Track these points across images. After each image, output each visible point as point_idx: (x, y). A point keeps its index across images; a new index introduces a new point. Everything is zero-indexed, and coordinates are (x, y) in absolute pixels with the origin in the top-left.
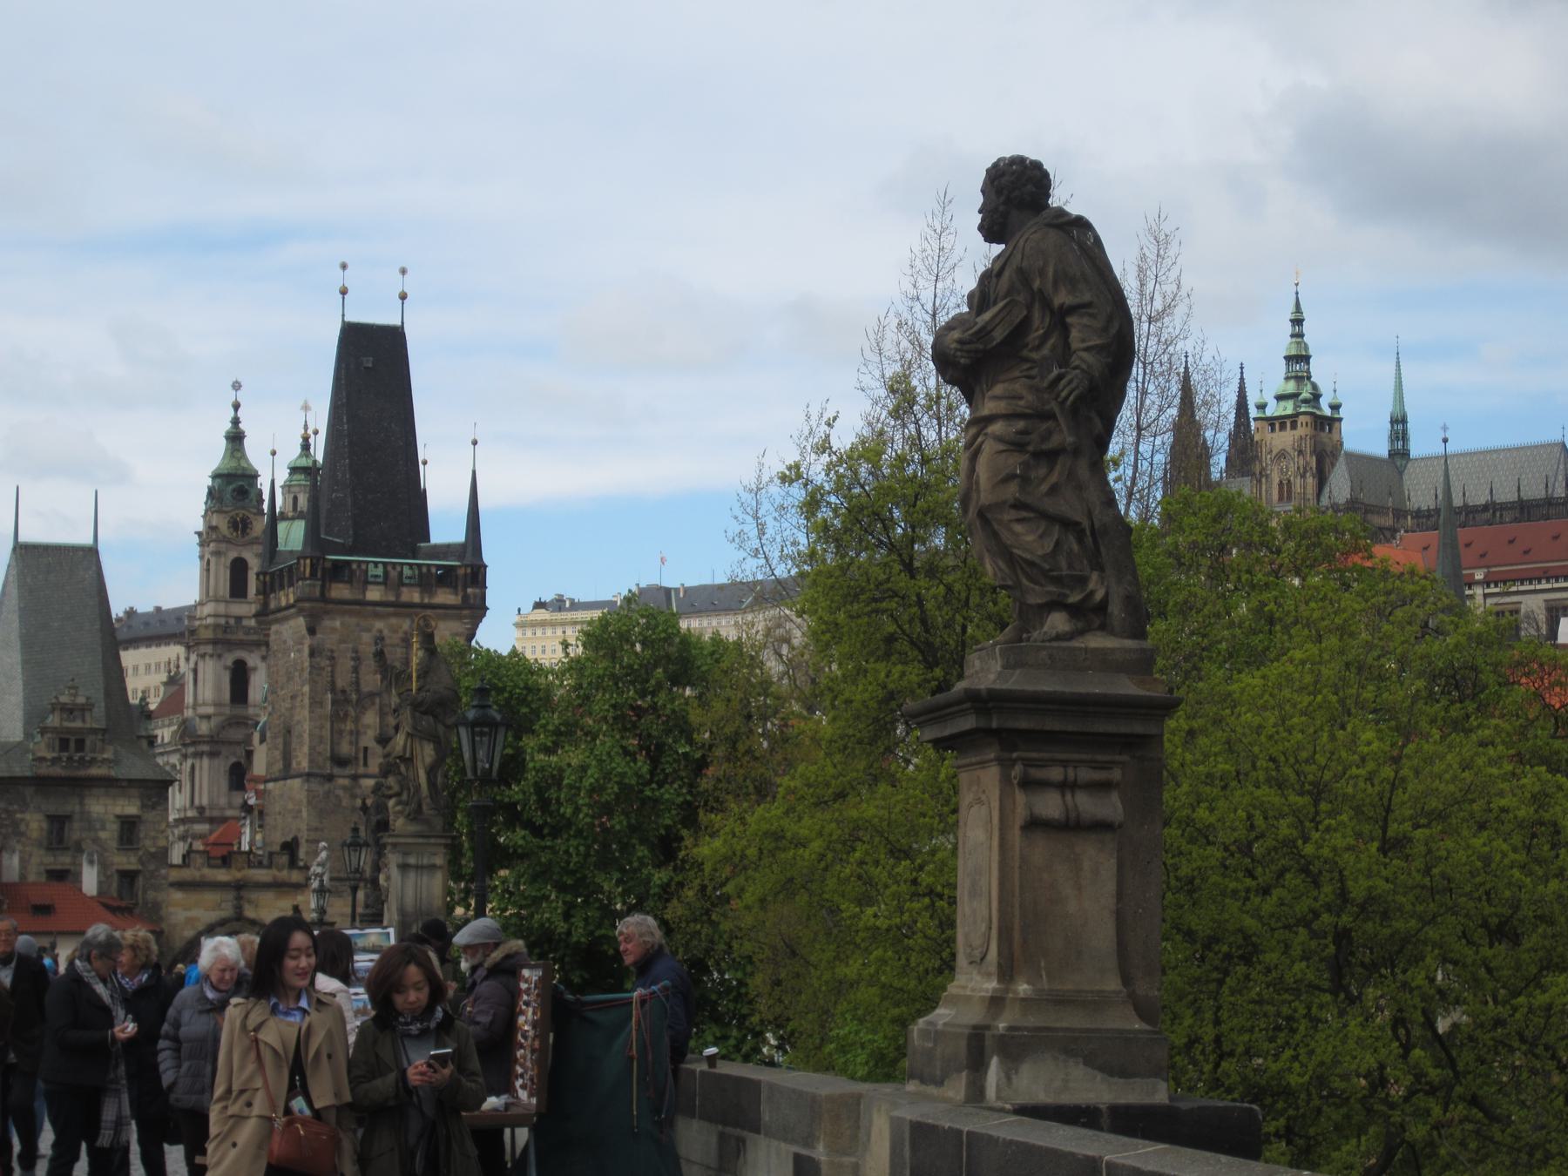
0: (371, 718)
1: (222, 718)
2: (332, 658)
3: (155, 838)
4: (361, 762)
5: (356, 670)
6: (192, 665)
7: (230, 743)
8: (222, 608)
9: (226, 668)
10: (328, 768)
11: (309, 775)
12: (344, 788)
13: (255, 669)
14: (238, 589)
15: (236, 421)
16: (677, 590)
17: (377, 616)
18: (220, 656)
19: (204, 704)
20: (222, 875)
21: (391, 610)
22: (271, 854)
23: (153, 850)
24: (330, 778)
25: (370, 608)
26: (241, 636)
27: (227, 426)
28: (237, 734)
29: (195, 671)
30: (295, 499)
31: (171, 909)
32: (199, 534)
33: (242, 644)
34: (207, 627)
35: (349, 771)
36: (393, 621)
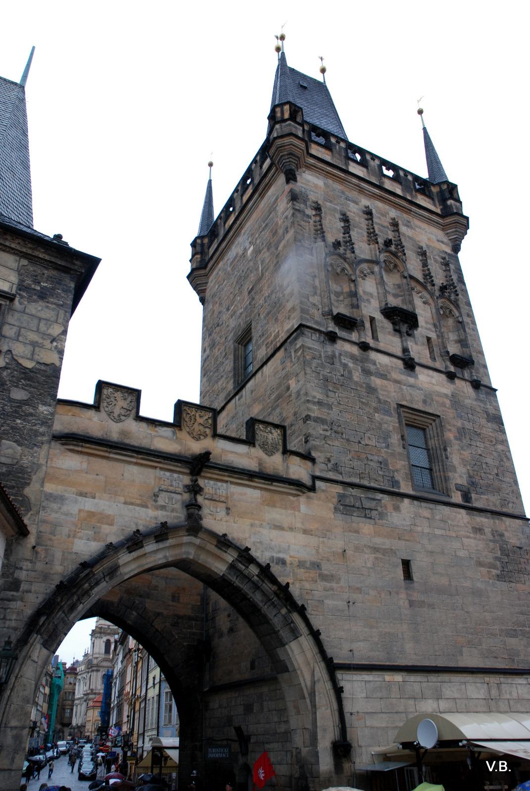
0: (368, 286)
2: (318, 208)
3: (34, 344)
4: (369, 333)
5: (347, 230)
10: (332, 327)
11: (301, 326)
12: (352, 357)
17: (361, 191)
20: (164, 442)
21: (377, 191)
22: (252, 424)
23: (29, 365)
24: (332, 338)
25: (355, 181)
31: (49, 488)
35: (354, 336)
36: (379, 204)
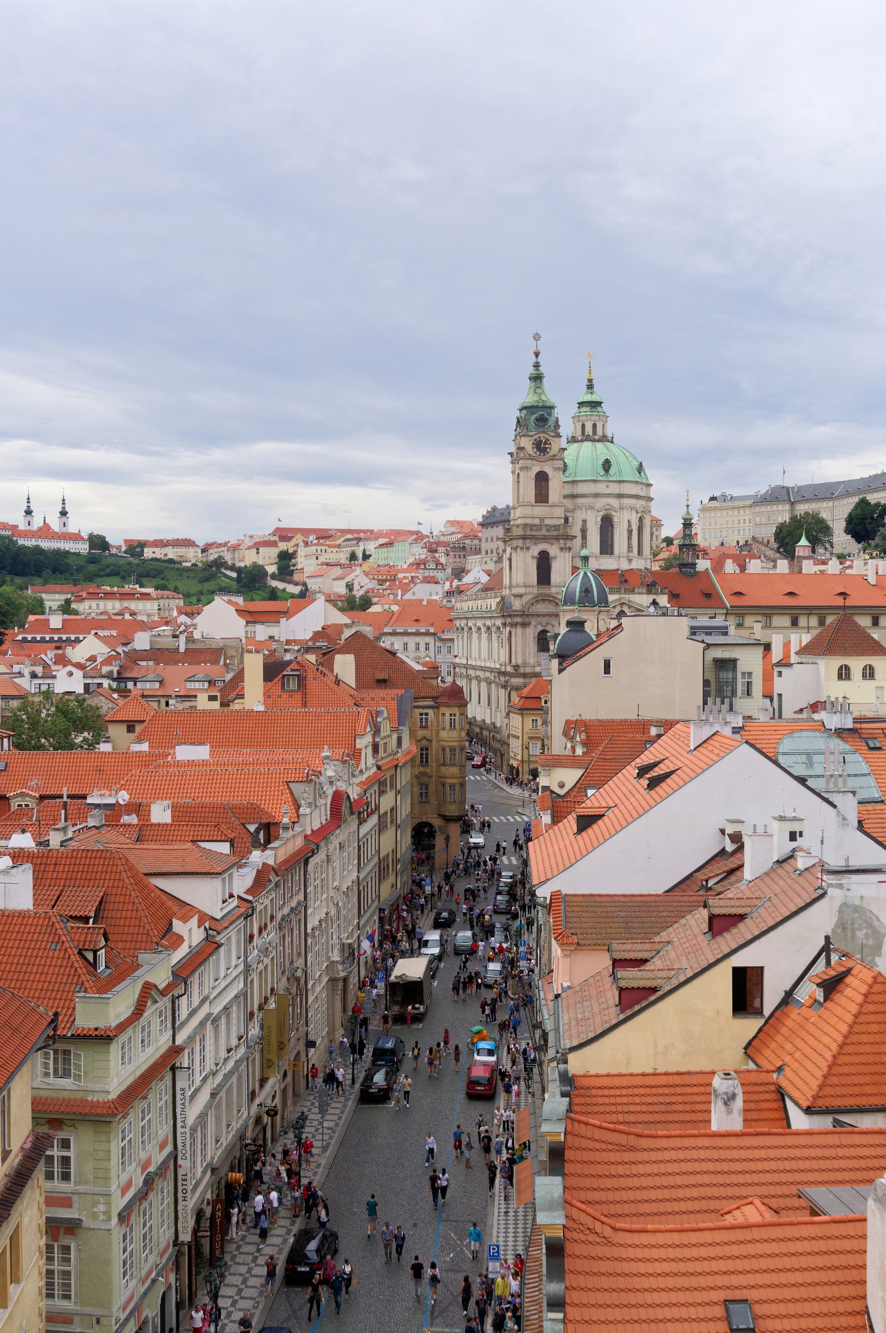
1: (532, 596)
6: (508, 556)
7: (538, 616)
8: (528, 511)
9: (533, 558)
13: (555, 558)
14: (542, 496)
15: (537, 366)
16: (793, 488)
18: (528, 548)
19: (517, 586)
26: (544, 532)
27: (532, 370)
28: (541, 608)
29: (510, 560)
30: (583, 426)
32: (511, 454)
33: (545, 539)
34: (518, 526)
